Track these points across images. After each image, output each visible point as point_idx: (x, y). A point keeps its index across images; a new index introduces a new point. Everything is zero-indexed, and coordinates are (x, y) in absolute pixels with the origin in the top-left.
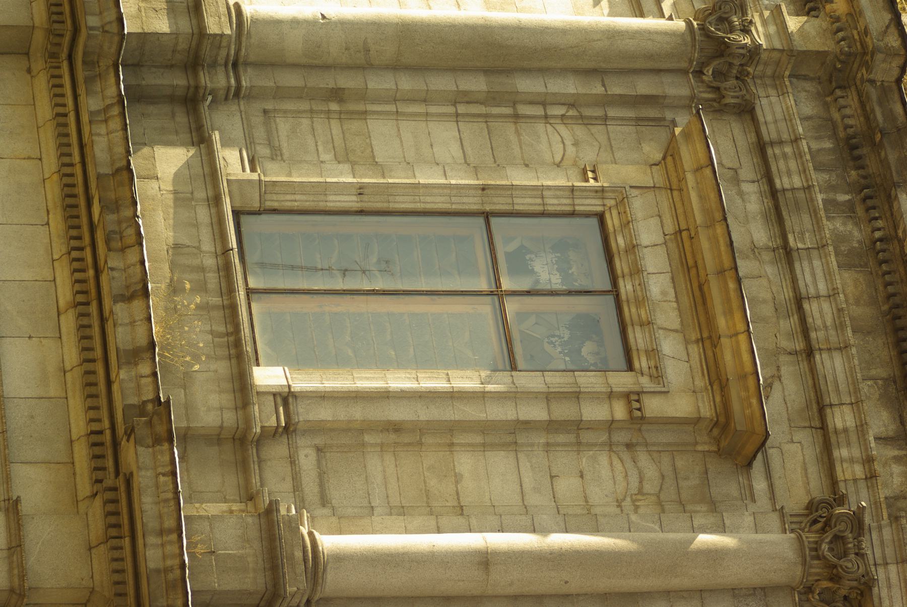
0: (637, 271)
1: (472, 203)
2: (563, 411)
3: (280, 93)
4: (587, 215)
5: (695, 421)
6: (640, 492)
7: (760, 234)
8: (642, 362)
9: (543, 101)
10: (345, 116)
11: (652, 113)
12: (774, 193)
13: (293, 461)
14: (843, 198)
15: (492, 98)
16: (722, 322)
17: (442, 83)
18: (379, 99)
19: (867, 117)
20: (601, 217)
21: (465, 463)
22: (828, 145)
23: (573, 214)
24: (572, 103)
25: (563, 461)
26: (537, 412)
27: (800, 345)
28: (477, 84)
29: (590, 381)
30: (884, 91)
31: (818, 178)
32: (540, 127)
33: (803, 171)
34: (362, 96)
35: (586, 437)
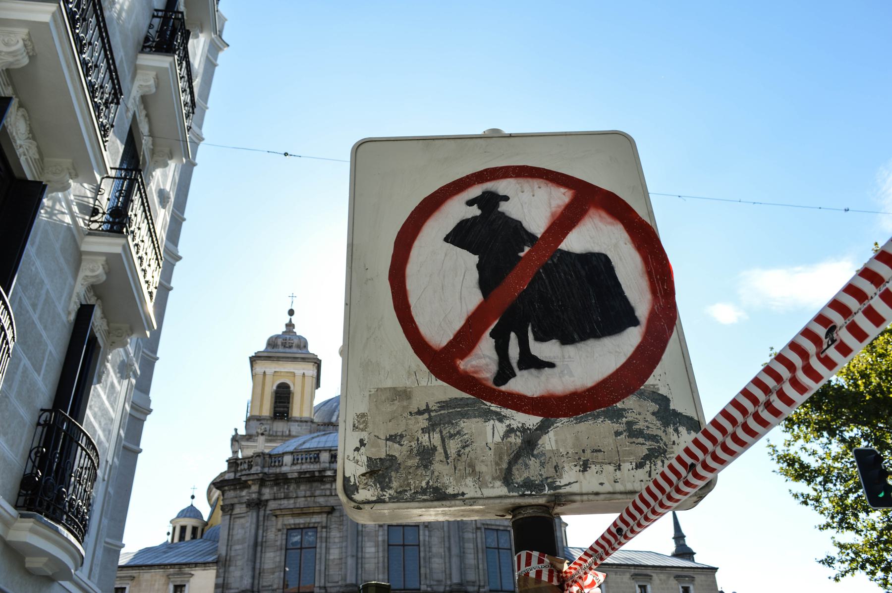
0: (299, 524)
1: (283, 552)
2: (324, 540)
3: (259, 584)
4: (287, 532)
5: (327, 517)
6: (338, 528)
7: (292, 501)
8: (316, 525)
9: (263, 537)
10: (263, 572)
11: (266, 518)
12: (284, 498)
13: (331, 587)
14: (286, 487)
15: (262, 546)
16: (311, 511)
17: (258, 555)
18: (260, 566)
19: (271, 480)
20: (288, 529)
21: (331, 557)
22: (275, 488)
23: (287, 534)
24: (263, 532)
25: (332, 540)
26: (324, 545)
27: (313, 498)
28: (259, 548)
29: (319, 535)
30: (268, 477)
31: (282, 490)
32: (268, 537)
33: (281, 493)
34: (260, 569)
35: (328, 536)
